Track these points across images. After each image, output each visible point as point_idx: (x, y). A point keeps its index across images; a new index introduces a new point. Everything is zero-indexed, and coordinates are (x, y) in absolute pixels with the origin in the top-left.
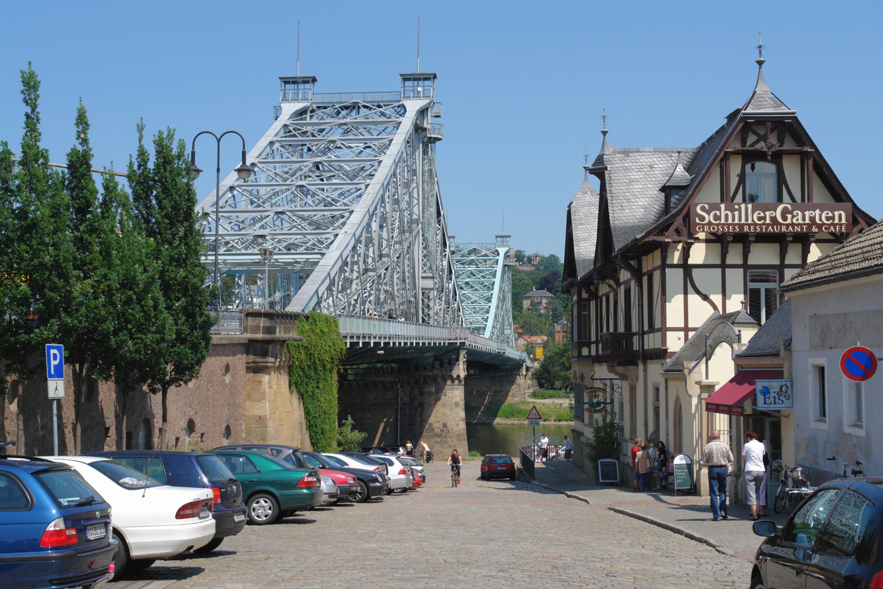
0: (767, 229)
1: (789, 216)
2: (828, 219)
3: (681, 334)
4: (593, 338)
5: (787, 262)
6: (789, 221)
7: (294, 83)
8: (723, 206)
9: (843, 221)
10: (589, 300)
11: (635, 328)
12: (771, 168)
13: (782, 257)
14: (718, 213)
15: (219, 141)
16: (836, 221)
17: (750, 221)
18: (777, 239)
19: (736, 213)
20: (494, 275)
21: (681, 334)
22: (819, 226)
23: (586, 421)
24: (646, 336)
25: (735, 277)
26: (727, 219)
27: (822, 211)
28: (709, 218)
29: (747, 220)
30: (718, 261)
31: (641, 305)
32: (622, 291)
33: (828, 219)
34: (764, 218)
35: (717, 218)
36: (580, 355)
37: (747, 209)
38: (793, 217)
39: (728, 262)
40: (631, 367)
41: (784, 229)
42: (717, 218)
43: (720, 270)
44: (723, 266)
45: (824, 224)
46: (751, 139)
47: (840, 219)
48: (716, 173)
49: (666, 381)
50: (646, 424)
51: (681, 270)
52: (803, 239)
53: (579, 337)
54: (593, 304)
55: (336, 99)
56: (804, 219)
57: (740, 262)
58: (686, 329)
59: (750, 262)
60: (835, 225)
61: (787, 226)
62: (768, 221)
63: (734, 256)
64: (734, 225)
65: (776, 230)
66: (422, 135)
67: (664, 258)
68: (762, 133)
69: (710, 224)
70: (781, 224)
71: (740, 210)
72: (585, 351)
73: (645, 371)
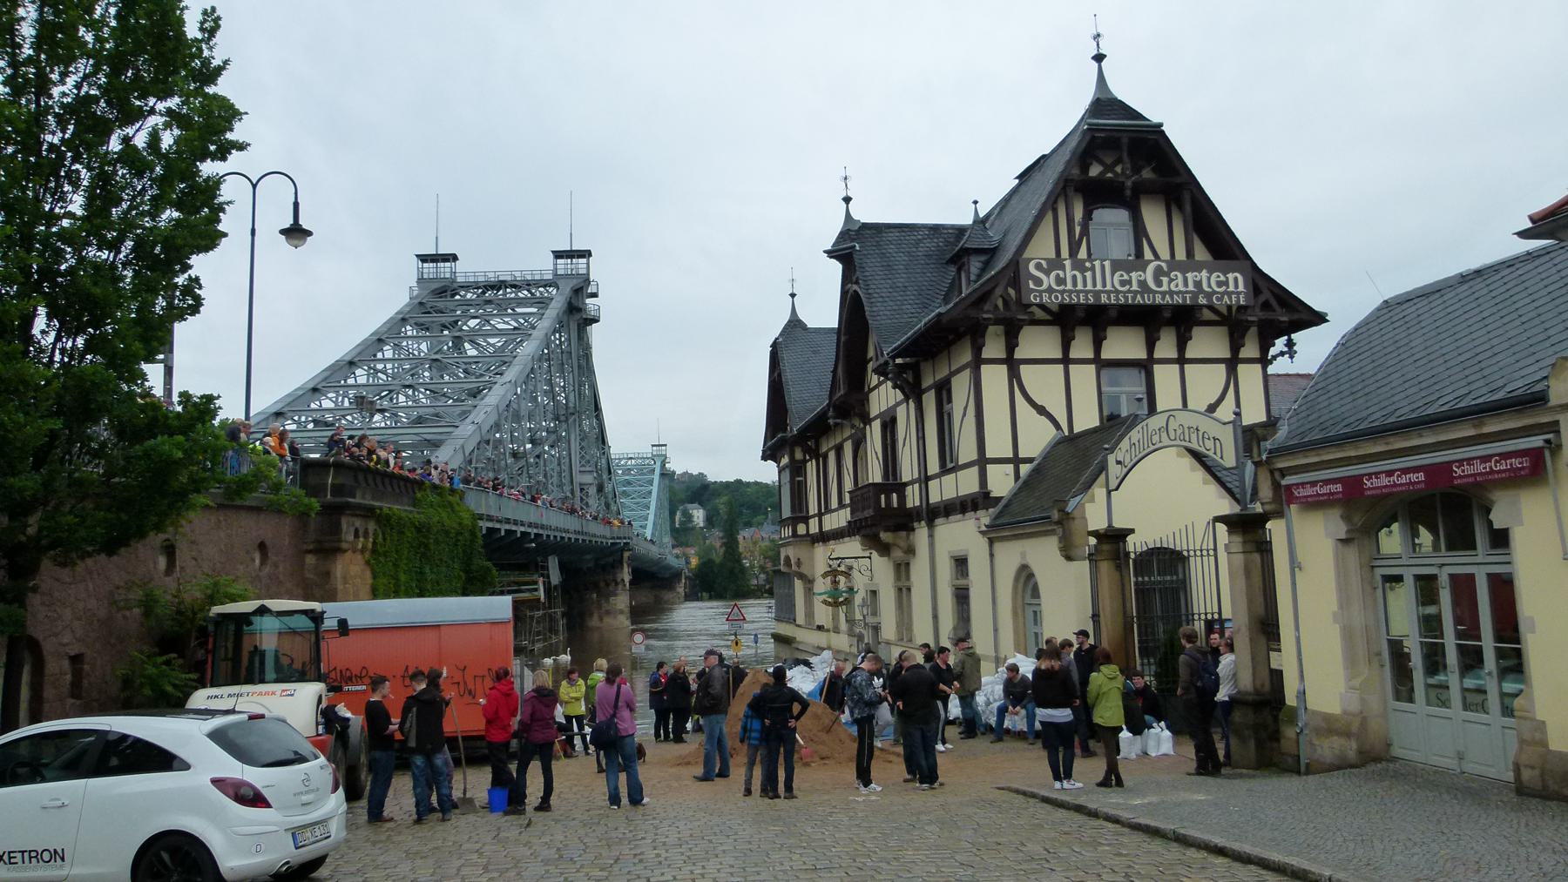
0: (1134, 298)
1: (1165, 280)
2: (1219, 284)
3: (1010, 468)
4: (813, 509)
5: (1156, 356)
6: (1165, 288)
7: (433, 261)
8: (1068, 263)
9: (1241, 288)
10: (805, 462)
11: (908, 471)
12: (1121, 216)
13: (1151, 347)
14: (1061, 274)
15: (254, 186)
17: (1109, 287)
18: (1146, 318)
19: (1088, 274)
20: (651, 482)
21: (1010, 468)
22: (1209, 295)
23: (800, 619)
25: (1084, 377)
27: (1211, 272)
28: (1049, 281)
29: (1104, 285)
30: (1059, 355)
31: (921, 438)
32: (875, 432)
33: (1219, 284)
34: (1129, 282)
36: (795, 534)
37: (1103, 267)
39: (1072, 355)
40: (904, 533)
41: (1158, 300)
43: (1061, 367)
44: (1066, 361)
45: (1215, 292)
46: (1095, 170)
47: (1236, 286)
48: (1049, 217)
49: (991, 542)
50: (935, 617)
51: (1004, 367)
52: (1183, 319)
54: (811, 468)
55: (481, 279)
56: (1186, 285)
57: (1091, 355)
58: (1016, 461)
59: (1103, 356)
60: (1229, 294)
61: (1163, 294)
62: (1135, 287)
63: (1082, 347)
64: (1087, 292)
65: (1148, 300)
66: (577, 316)
67: (977, 350)
69: (1050, 290)
71: (1093, 269)
72: (801, 529)
73: (931, 536)
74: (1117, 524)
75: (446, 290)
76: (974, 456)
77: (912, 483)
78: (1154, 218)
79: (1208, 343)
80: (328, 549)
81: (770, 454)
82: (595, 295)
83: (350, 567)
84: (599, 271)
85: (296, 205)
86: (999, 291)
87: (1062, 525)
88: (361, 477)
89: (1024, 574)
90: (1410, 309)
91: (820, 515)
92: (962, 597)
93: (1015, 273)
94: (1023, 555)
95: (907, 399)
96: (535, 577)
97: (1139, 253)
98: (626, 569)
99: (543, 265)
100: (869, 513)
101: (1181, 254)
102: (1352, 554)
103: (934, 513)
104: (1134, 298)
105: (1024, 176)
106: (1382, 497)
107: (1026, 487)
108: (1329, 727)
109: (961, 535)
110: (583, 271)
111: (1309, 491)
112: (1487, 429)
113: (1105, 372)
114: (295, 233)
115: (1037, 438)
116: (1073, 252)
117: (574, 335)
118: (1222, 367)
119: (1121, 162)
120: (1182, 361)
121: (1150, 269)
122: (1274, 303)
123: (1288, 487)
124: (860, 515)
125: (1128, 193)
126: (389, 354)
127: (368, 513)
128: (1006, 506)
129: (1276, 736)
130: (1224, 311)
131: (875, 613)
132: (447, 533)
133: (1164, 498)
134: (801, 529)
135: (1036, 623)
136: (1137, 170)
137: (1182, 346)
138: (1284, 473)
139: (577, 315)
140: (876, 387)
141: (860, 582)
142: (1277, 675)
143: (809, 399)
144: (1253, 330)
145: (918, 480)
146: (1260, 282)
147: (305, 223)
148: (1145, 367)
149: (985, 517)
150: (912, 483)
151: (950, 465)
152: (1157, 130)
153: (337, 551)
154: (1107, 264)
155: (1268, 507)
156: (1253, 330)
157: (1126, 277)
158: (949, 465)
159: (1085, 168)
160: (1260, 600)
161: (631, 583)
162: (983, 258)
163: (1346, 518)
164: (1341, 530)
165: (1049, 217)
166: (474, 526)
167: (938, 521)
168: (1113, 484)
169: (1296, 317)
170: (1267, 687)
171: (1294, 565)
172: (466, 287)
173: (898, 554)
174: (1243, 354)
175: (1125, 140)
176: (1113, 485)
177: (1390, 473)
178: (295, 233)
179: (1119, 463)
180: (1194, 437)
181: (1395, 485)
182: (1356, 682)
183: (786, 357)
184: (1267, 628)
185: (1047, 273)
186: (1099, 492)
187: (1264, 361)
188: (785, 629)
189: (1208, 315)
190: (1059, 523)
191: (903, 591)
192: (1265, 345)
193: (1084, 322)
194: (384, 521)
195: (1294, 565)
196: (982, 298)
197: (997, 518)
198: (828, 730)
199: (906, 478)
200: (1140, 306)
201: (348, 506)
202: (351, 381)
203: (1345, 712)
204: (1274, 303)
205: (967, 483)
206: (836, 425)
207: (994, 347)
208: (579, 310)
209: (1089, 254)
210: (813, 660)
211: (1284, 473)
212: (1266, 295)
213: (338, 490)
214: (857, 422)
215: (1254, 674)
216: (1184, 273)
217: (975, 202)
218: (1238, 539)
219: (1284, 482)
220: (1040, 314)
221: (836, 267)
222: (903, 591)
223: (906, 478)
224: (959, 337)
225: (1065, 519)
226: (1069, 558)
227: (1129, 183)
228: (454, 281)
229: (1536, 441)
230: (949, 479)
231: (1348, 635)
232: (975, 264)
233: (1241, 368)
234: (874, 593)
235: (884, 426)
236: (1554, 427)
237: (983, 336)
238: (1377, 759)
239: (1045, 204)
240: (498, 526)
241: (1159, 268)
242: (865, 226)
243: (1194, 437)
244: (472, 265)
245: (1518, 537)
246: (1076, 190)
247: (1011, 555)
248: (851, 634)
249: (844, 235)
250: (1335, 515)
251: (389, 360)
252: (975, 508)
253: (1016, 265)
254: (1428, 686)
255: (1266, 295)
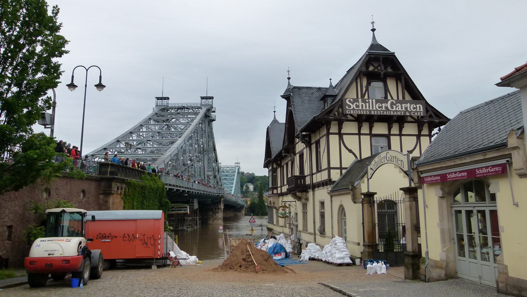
0: (383, 113)
1: (394, 106)
2: (414, 108)
3: (339, 171)
4: (279, 185)
5: (391, 133)
6: (394, 109)
7: (161, 99)
8: (360, 100)
9: (422, 110)
10: (277, 168)
11: (307, 172)
12: (380, 84)
13: (390, 130)
15: (87, 70)
16: (418, 110)
17: (374, 109)
18: (388, 120)
19: (367, 104)
20: (234, 175)
21: (339, 171)
22: (410, 112)
23: (275, 223)
24: (314, 176)
25: (366, 140)
26: (362, 107)
28: (353, 106)
29: (373, 108)
31: (311, 160)
32: (297, 158)
33: (414, 108)
34: (382, 107)
35: (357, 106)
36: (273, 193)
37: (372, 102)
38: (396, 107)
41: (392, 113)
42: (357, 106)
44: (359, 134)
45: (412, 111)
46: (371, 68)
47: (420, 109)
48: (354, 84)
49: (331, 197)
50: (314, 223)
51: (338, 136)
52: (401, 120)
53: (272, 185)
54: (279, 170)
56: (402, 108)
58: (341, 168)
59: (373, 132)
60: (417, 112)
61: (394, 111)
62: (384, 109)
63: (365, 129)
65: (388, 113)
66: (208, 119)
67: (328, 130)
68: (376, 65)
69: (354, 109)
70: (391, 111)
71: (369, 102)
73: (314, 194)
74: (371, 191)
75: (165, 109)
76: (327, 167)
77: (308, 176)
78: (392, 85)
79: (410, 129)
80: (108, 193)
81: (266, 166)
82: (214, 112)
83: (115, 199)
84: (216, 103)
85: (100, 77)
86: (336, 109)
87: (353, 190)
88: (121, 169)
89: (341, 208)
90: (468, 115)
91: (281, 187)
92: (322, 215)
93: (341, 104)
94: (341, 201)
95: (307, 147)
96: (186, 205)
97: (386, 97)
98: (222, 204)
99: (198, 101)
100: (293, 186)
101: (401, 98)
102: (444, 202)
103: (315, 186)
104: (383, 113)
105: (348, 72)
106: (454, 181)
107: (344, 177)
108: (436, 265)
109: (322, 194)
110: (211, 104)
111: (429, 179)
112: (487, 157)
113: (373, 138)
114: (100, 86)
115: (348, 160)
116: (363, 96)
117: (207, 124)
118: (415, 138)
119: (380, 66)
120: (401, 135)
121: (389, 102)
122: (433, 115)
123: (423, 178)
124: (291, 187)
125: (382, 76)
126: (144, 130)
127: (123, 181)
128: (337, 184)
129: (418, 268)
130: (416, 118)
131: (297, 221)
132: (153, 189)
133: (387, 181)
134: (275, 192)
135: (345, 225)
136: (386, 68)
137: (401, 129)
138: (422, 172)
139: (208, 118)
140: (298, 142)
141: (293, 210)
142: (420, 245)
143: (277, 147)
144: (426, 125)
145: (310, 175)
146: (428, 107)
147: (103, 83)
148: (388, 137)
149: (330, 188)
150: (308, 176)
151: (319, 170)
152: (393, 55)
153: (111, 194)
154: (374, 101)
155: (417, 185)
156: (426, 125)
157: (380, 105)
158: (319, 170)
159: (367, 67)
160: (415, 218)
161: (224, 209)
162: (332, 98)
163: (442, 189)
164: (440, 194)
165: (354, 84)
166: (163, 187)
167: (316, 189)
168: (369, 177)
169: (441, 120)
170: (417, 250)
171: (425, 206)
172: (172, 108)
173: (303, 200)
174: (423, 133)
175: (381, 58)
176: (369, 177)
177: (455, 173)
178: (100, 86)
179: (371, 169)
180: (395, 160)
181: (457, 177)
182: (445, 249)
183: (270, 132)
184: (417, 228)
185: (353, 103)
186: (365, 179)
187: (430, 136)
188: (270, 226)
189: (410, 119)
190: (352, 190)
191: (305, 213)
192: (430, 131)
193: (366, 121)
194: (129, 184)
195: (425, 206)
196: (330, 111)
197: (333, 188)
198: (266, 260)
199: (306, 175)
200: (385, 115)
201: (115, 178)
202: (131, 138)
203: (441, 260)
204: (433, 115)
205: (323, 176)
206: (285, 156)
207: (334, 129)
208: (209, 117)
209: (368, 97)
210: (277, 237)
211: (422, 172)
212: (431, 113)
213: (112, 173)
214: (292, 155)
215: (412, 246)
216: (401, 104)
217: (331, 79)
218: (408, 196)
219: (422, 176)
220: (350, 117)
221: (285, 102)
222: (305, 213)
223: (306, 174)
224: (323, 125)
225: (354, 189)
226: (355, 203)
227: (382, 73)
228: (168, 106)
229: (504, 161)
230: (319, 174)
231: (442, 232)
232: (329, 100)
233: (422, 138)
234: (297, 214)
235: (300, 156)
236: (510, 156)
237: (330, 125)
238: (452, 278)
239: (352, 79)
240: (173, 188)
241: (392, 102)
242: (295, 87)
243: (395, 160)
244: (174, 101)
245: (499, 197)
246: (364, 75)
247: (338, 201)
248: (290, 228)
249: (287, 90)
250: (438, 187)
251: (144, 132)
252: (327, 185)
253: (342, 100)
254: (470, 251)
255: (431, 113)
